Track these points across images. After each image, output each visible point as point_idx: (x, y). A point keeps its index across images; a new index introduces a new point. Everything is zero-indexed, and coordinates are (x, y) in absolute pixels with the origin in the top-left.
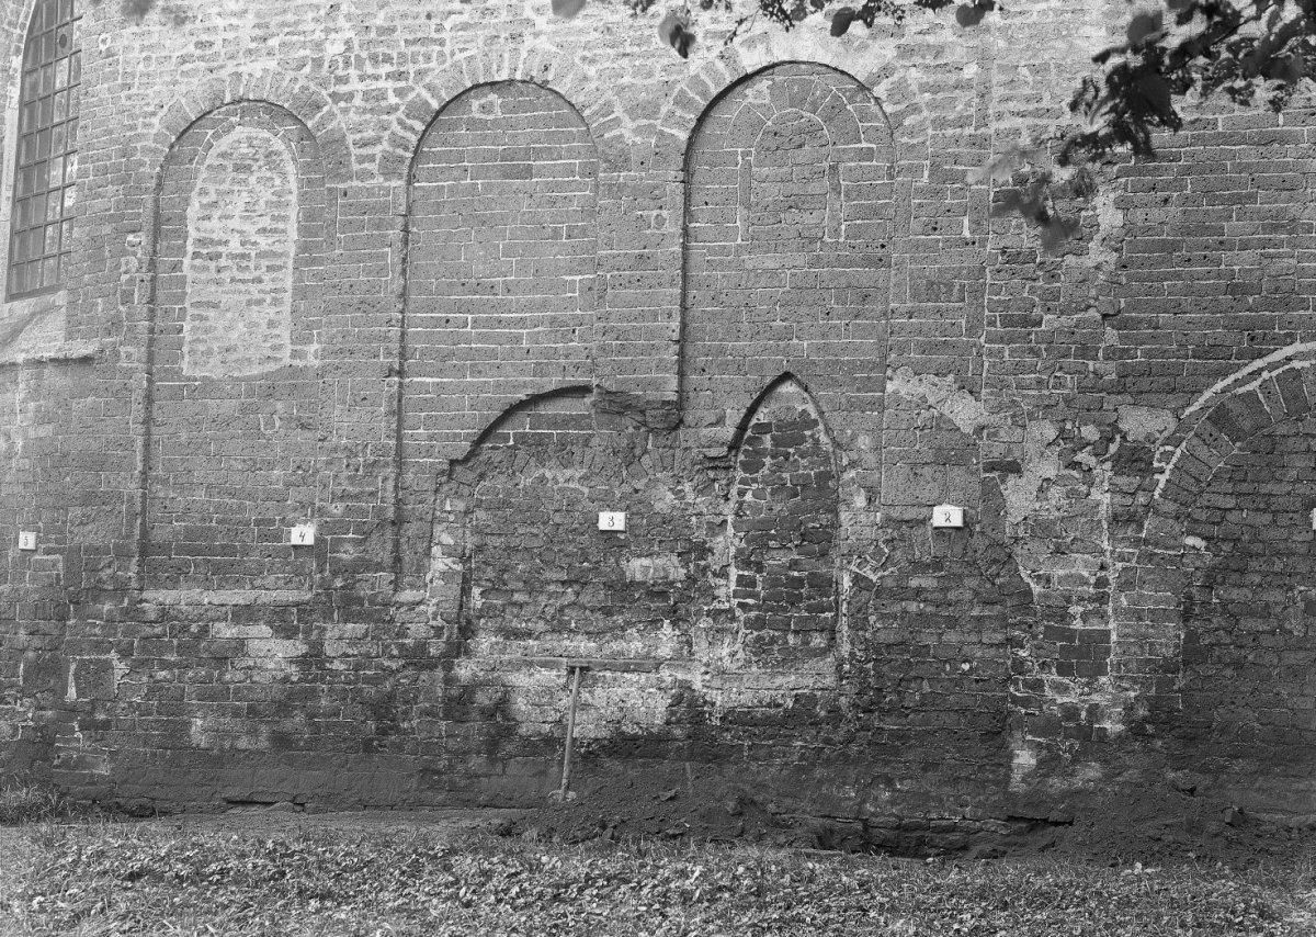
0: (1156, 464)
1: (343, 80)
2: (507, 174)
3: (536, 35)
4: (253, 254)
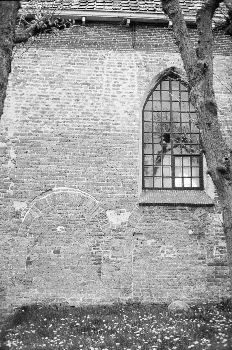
0: (22, 216)
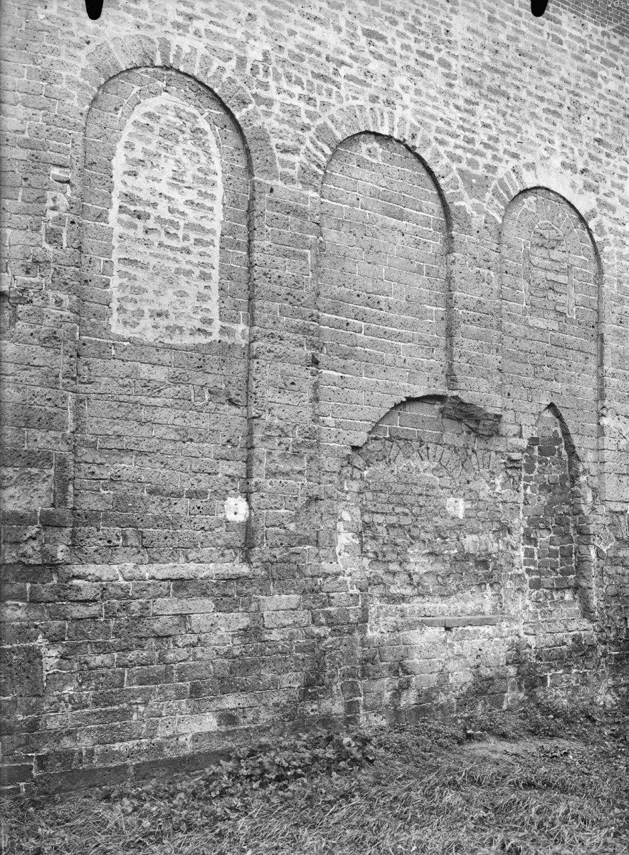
1: (265, 86)
3: (405, 107)
4: (182, 223)
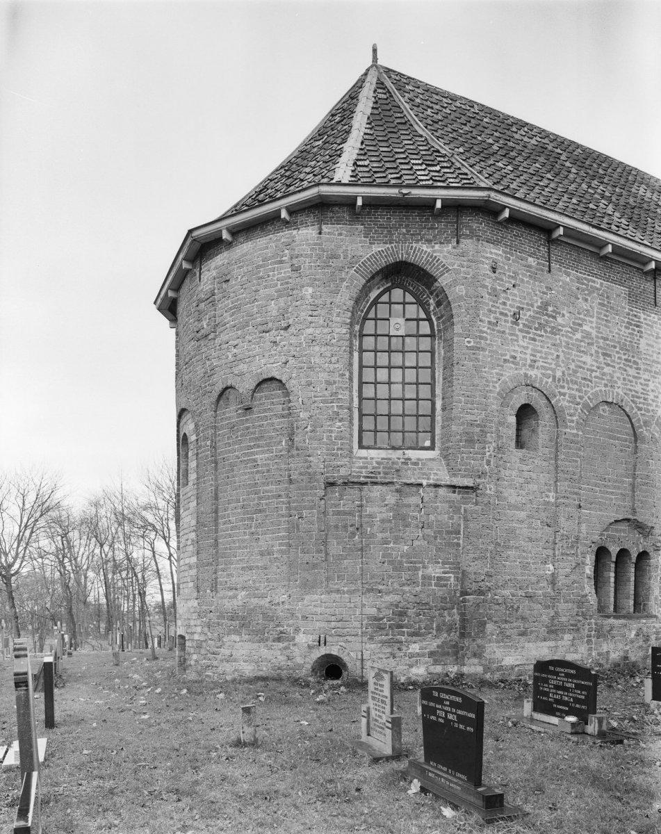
2: (610, 437)
3: (619, 388)
